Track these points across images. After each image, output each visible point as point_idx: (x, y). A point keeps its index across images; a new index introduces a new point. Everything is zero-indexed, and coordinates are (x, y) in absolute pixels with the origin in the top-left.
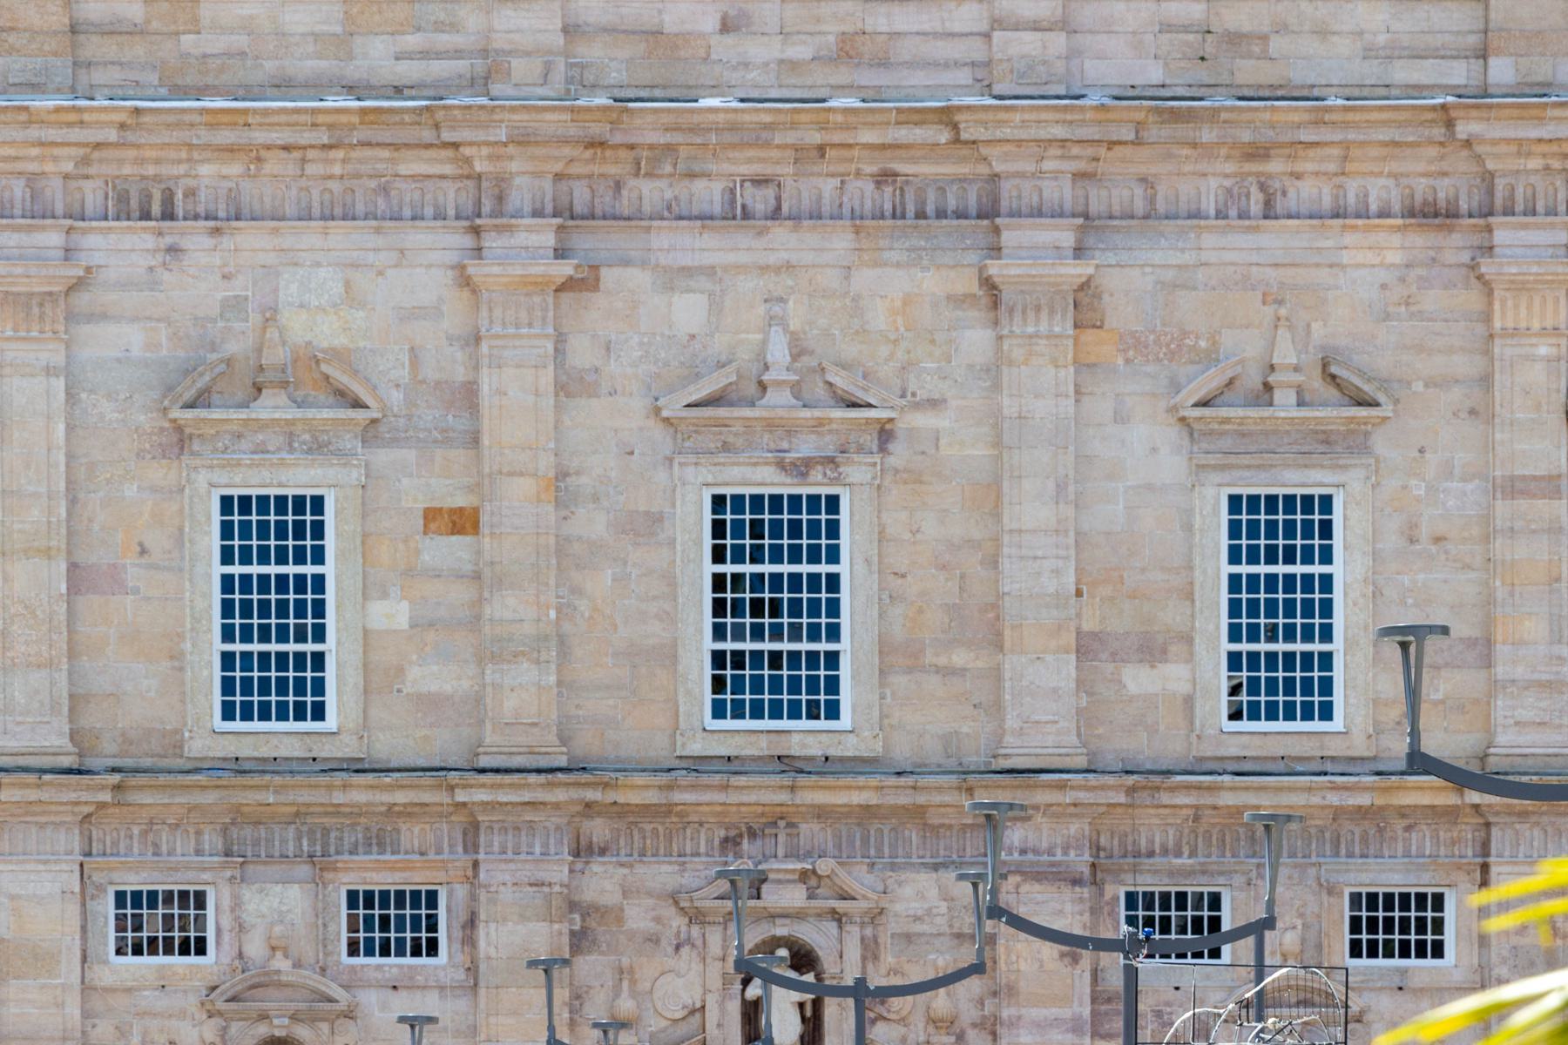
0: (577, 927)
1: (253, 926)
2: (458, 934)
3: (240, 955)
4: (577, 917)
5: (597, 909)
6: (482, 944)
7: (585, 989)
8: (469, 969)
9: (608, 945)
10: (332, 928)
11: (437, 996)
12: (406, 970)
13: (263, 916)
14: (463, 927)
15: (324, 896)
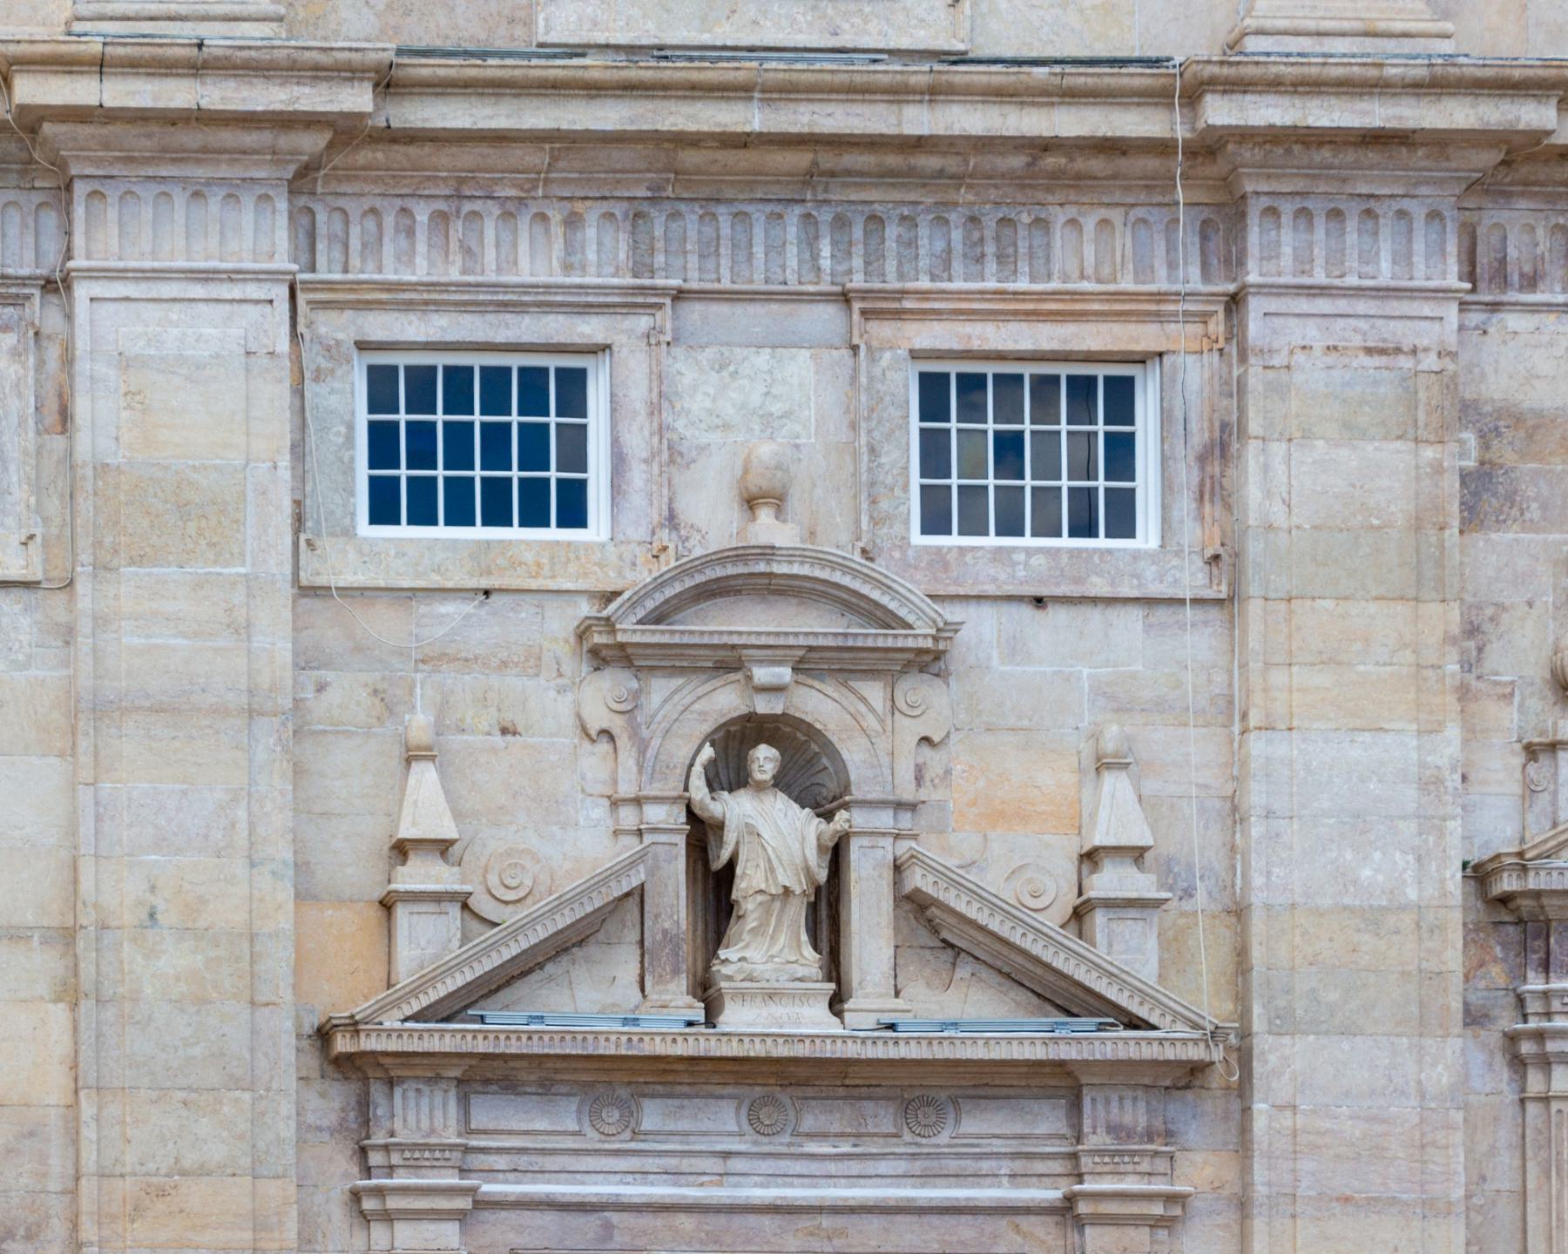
0: (1471, 464)
1: (702, 449)
2: (1188, 476)
3: (671, 520)
4: (1470, 437)
5: (1518, 419)
6: (1253, 493)
7: (1489, 611)
8: (1216, 558)
9: (1544, 507)
10: (889, 457)
11: (1139, 626)
12: (1065, 559)
13: (726, 427)
14: (1202, 459)
15: (871, 379)
